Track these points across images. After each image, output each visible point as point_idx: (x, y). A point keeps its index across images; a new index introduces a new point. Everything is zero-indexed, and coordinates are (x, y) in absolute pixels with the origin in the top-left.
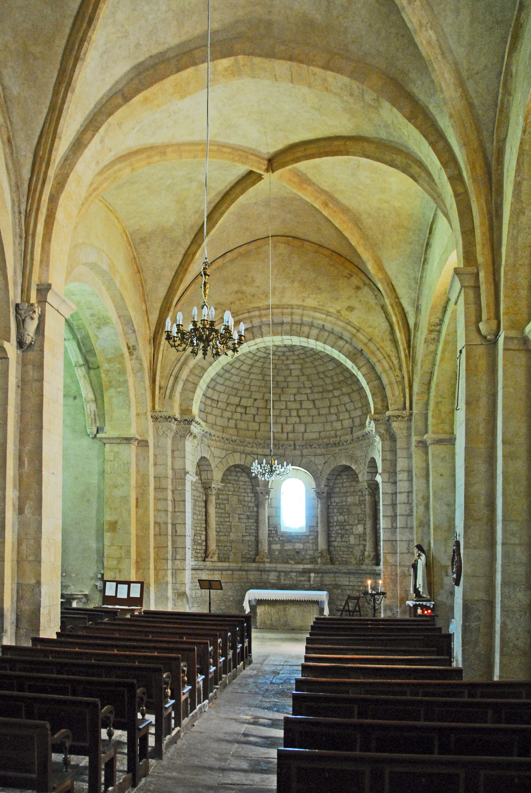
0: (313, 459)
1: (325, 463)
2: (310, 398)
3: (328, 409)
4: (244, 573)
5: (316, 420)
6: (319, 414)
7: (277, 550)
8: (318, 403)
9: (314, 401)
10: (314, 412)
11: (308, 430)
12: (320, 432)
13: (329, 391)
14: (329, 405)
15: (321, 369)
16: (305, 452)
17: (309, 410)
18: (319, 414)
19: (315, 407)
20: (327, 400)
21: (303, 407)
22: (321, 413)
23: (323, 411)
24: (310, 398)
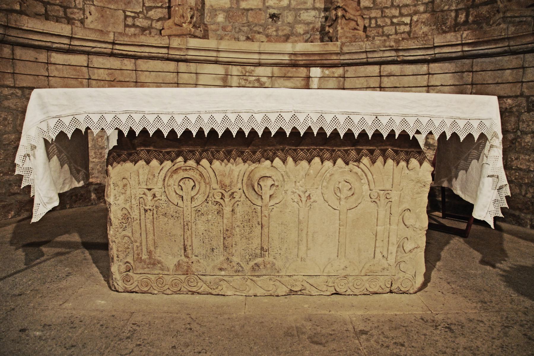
4: (129, 64)
7: (223, 10)
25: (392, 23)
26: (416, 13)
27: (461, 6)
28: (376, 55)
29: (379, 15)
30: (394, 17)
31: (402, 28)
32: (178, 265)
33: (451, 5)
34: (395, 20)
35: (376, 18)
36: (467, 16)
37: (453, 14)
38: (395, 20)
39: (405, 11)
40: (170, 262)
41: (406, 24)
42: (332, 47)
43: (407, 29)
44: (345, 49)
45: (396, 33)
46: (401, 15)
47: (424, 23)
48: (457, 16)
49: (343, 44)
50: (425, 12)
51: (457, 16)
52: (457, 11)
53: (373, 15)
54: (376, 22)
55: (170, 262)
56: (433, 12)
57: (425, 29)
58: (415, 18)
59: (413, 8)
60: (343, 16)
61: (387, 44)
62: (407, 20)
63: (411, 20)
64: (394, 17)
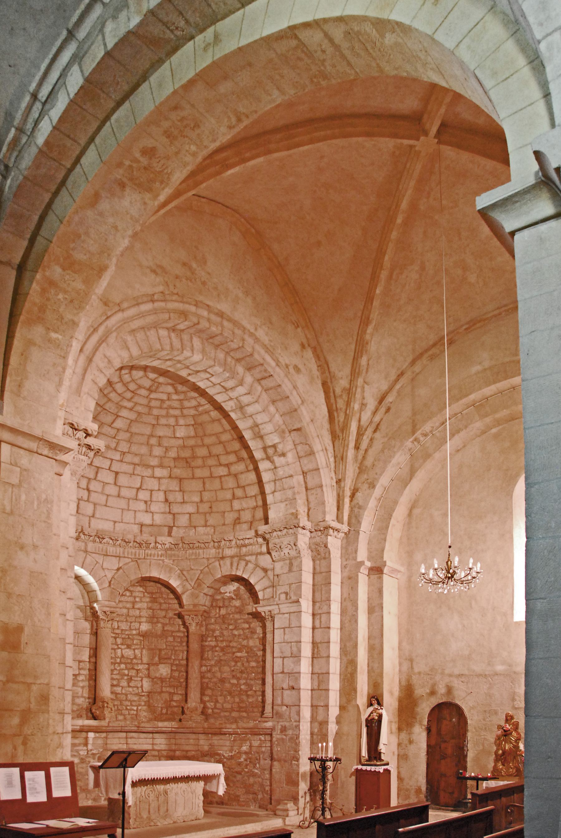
0: (100, 559)
1: (118, 569)
2: (113, 468)
3: (135, 491)
5: (112, 502)
6: (119, 496)
8: (123, 480)
9: (117, 473)
10: (112, 490)
11: (97, 515)
12: (115, 522)
13: (148, 466)
14: (138, 485)
15: (160, 432)
16: (91, 546)
17: (105, 484)
18: (119, 496)
19: (115, 484)
20: (140, 477)
21: (99, 478)
22: (122, 494)
23: (125, 492)
24: (113, 468)
25: (127, 709)
26: (140, 705)
27: (164, 706)
28: (126, 728)
29: (119, 703)
30: (128, 706)
31: (132, 712)
32: (147, 817)
33: (158, 704)
34: (128, 708)
35: (117, 705)
36: (167, 711)
37: (160, 709)
38: (128, 708)
39: (134, 703)
40: (145, 817)
41: (134, 710)
42: (104, 723)
43: (135, 713)
44: (110, 725)
45: (129, 714)
46: (132, 705)
47: (144, 711)
48: (162, 710)
49: (109, 722)
50: (145, 705)
51: (162, 710)
52: (162, 708)
53: (116, 703)
54: (118, 707)
55: (145, 817)
56: (149, 706)
57: (145, 714)
58: (140, 708)
59: (138, 703)
60: (107, 707)
61: (134, 723)
62: (135, 708)
63: (137, 708)
64: (128, 706)
